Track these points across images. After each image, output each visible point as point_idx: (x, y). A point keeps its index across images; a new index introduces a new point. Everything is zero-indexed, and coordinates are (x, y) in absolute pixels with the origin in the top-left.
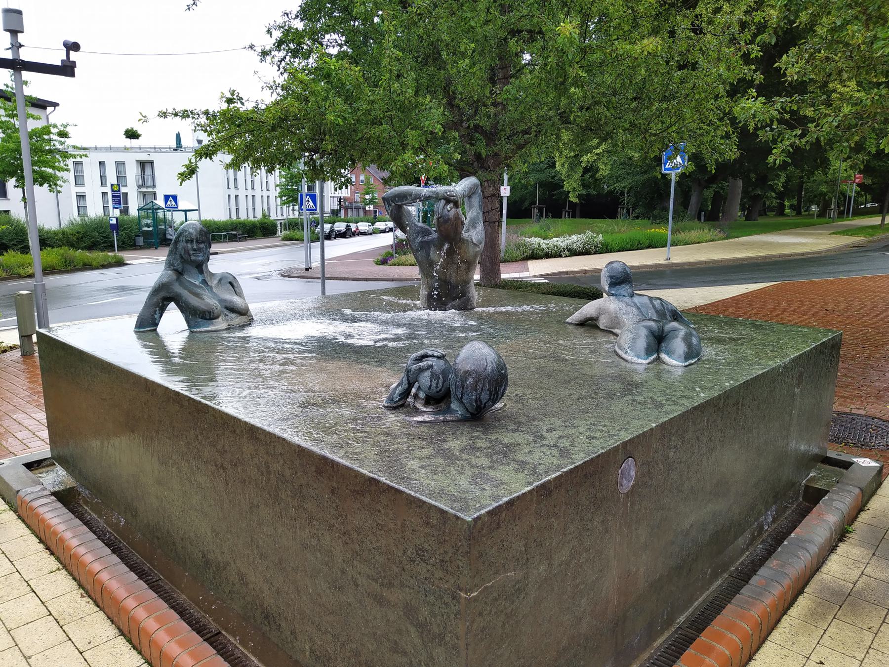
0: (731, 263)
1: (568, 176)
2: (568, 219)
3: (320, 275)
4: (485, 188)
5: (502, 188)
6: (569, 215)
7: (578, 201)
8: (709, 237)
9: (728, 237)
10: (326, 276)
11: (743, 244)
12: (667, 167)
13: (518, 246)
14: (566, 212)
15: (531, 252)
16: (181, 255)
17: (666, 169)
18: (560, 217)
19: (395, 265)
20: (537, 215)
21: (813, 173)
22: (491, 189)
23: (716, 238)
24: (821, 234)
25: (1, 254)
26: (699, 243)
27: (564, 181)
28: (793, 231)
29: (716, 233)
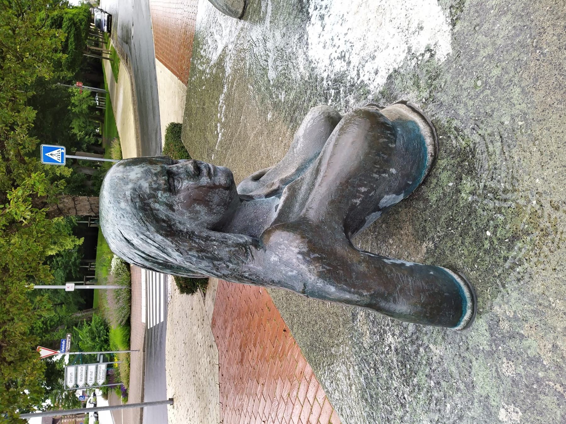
0: (137, 114)
1: (62, 246)
2: (96, 266)
3: (138, 408)
4: (65, 206)
5: (67, 290)
6: (93, 265)
7: (83, 238)
8: (118, 147)
9: (118, 137)
10: (139, 401)
11: (123, 124)
12: (60, 161)
13: (118, 274)
14: (90, 224)
15: (123, 264)
16: (148, 257)
17: (62, 162)
18: (94, 271)
19: (128, 382)
20: (92, 282)
21: (73, 104)
22: (67, 201)
23: (118, 142)
24: (117, 89)
25: (332, 423)
26: (121, 152)
27: (65, 249)
28: (114, 110)
29: (115, 144)
